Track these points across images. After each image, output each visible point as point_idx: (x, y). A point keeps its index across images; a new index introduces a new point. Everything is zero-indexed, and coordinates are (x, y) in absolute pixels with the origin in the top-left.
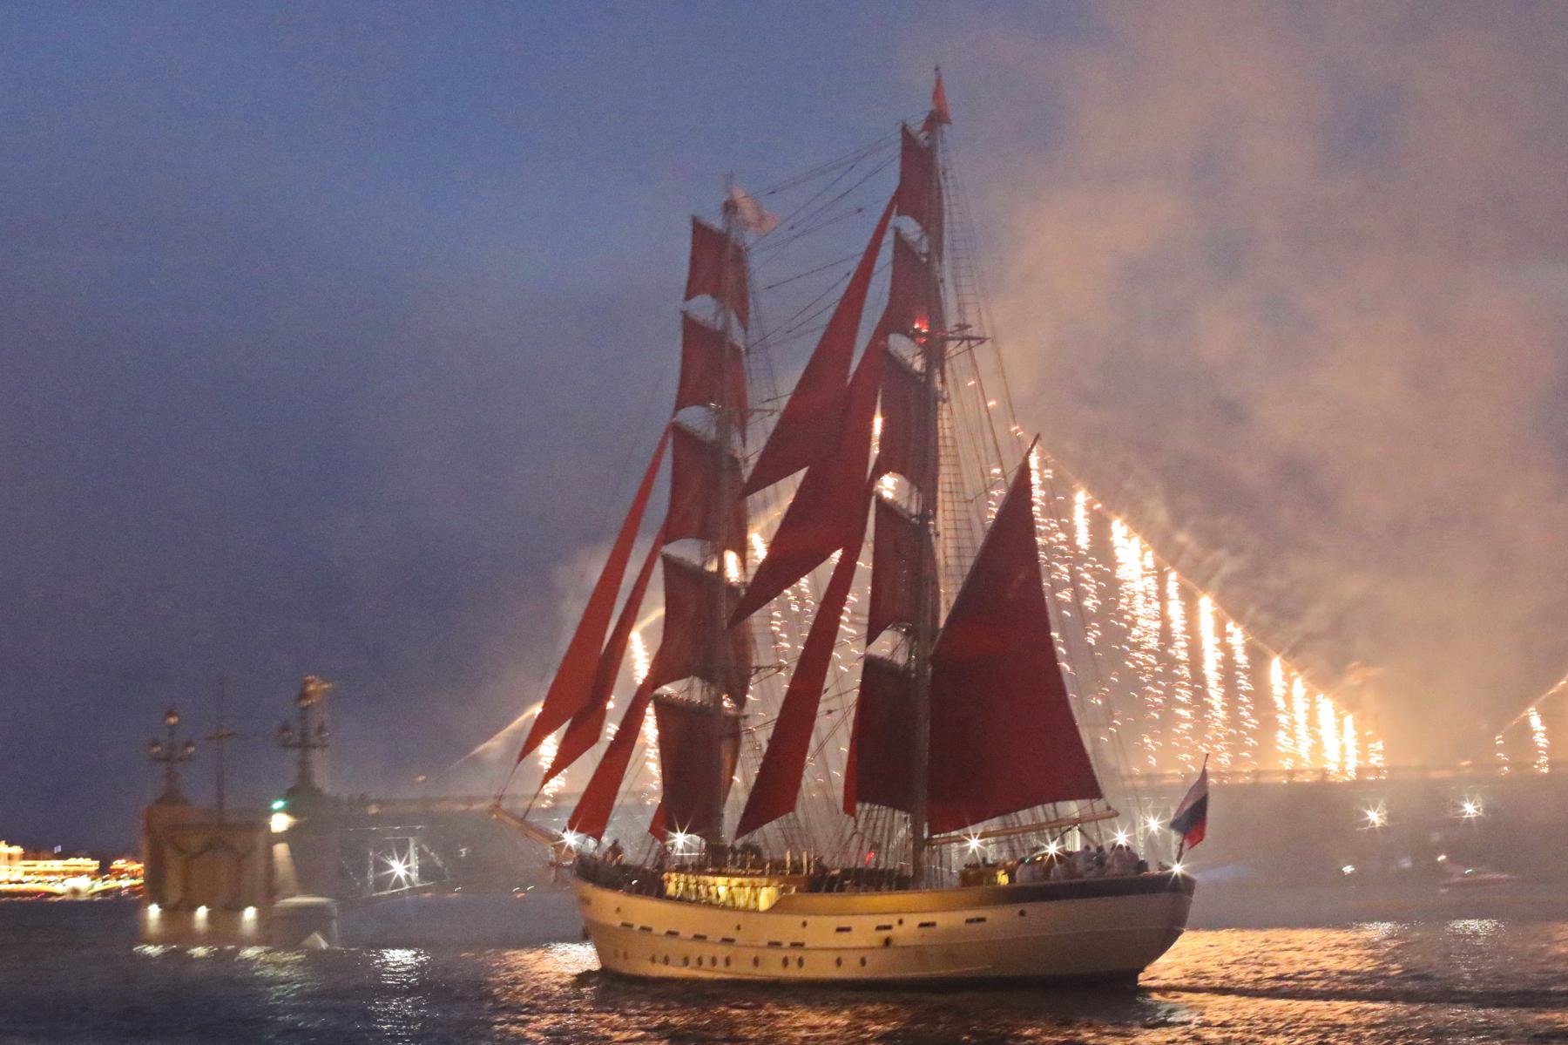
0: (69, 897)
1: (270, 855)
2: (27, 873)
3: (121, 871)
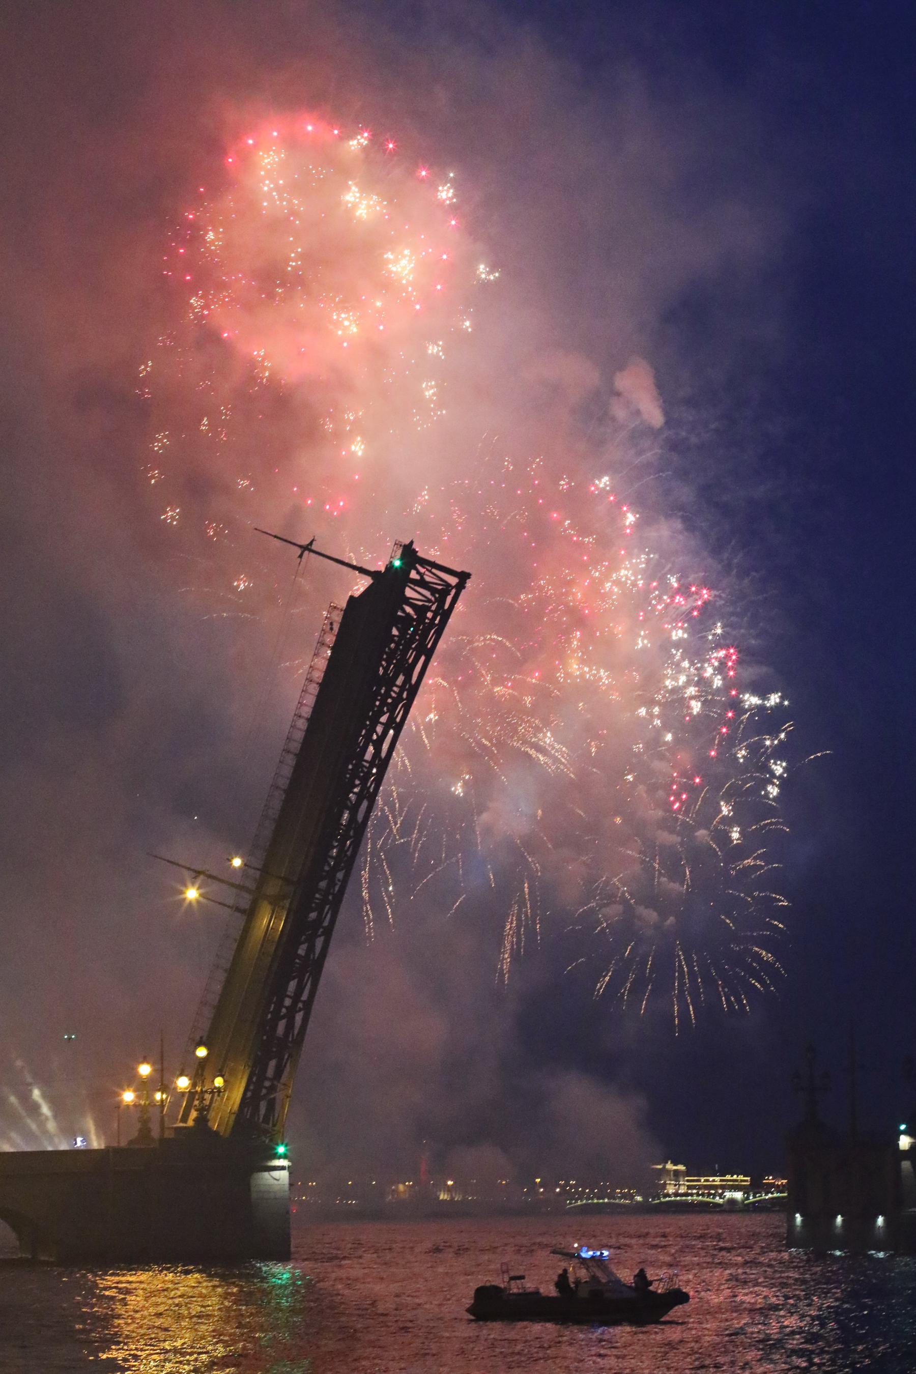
0: (727, 1207)
2: (689, 1187)
3: (773, 1185)
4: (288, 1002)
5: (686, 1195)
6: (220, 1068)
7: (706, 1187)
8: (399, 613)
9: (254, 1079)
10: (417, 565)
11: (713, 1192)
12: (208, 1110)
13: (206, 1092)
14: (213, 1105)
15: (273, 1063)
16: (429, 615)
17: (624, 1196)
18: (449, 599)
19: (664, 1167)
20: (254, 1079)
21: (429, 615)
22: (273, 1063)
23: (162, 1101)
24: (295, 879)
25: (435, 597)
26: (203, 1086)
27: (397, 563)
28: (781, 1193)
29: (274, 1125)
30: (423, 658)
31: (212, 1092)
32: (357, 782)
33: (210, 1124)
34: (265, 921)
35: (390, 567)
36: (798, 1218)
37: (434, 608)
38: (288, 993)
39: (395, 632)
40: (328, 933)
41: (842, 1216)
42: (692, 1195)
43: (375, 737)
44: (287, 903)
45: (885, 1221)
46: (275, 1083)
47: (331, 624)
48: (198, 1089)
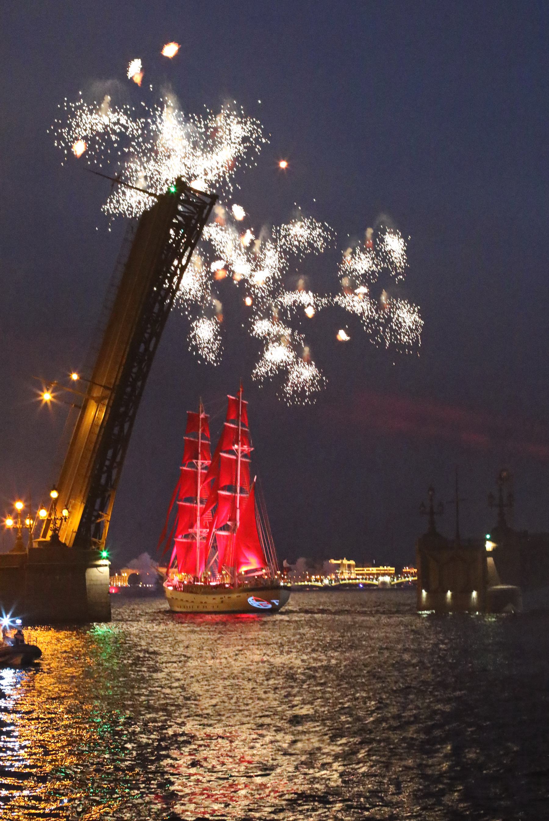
0: (381, 587)
1: (485, 561)
2: (357, 574)
3: (407, 573)
4: (107, 463)
5: (356, 579)
6: (66, 504)
7: (368, 574)
8: (174, 221)
9: (87, 511)
10: (186, 191)
11: (371, 577)
12: (59, 531)
13: (58, 519)
14: (62, 527)
15: (98, 501)
16: (193, 221)
17: (317, 580)
18: (206, 211)
19: (342, 562)
20: (87, 511)
21: (193, 221)
22: (98, 501)
23: (30, 525)
24: (112, 387)
25: (196, 210)
26: (55, 515)
27: (173, 190)
28: (414, 577)
29: (100, 538)
30: (189, 249)
31: (61, 519)
32: (149, 326)
33: (60, 539)
34: (93, 413)
35: (168, 192)
36: (424, 593)
37: (196, 217)
38: (108, 458)
39: (172, 232)
40: (132, 419)
41: (451, 591)
42: (359, 579)
43: (160, 298)
44: (106, 402)
45: (479, 595)
46: (100, 513)
47: (132, 228)
48: (53, 517)
